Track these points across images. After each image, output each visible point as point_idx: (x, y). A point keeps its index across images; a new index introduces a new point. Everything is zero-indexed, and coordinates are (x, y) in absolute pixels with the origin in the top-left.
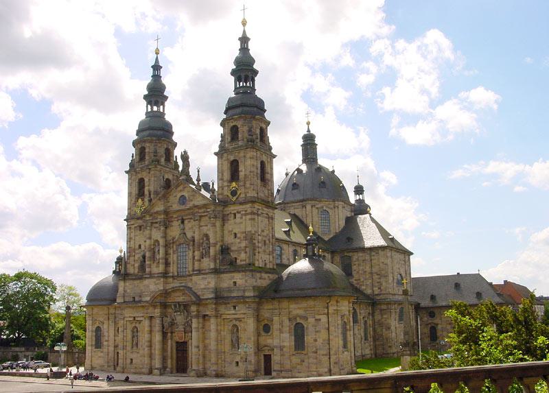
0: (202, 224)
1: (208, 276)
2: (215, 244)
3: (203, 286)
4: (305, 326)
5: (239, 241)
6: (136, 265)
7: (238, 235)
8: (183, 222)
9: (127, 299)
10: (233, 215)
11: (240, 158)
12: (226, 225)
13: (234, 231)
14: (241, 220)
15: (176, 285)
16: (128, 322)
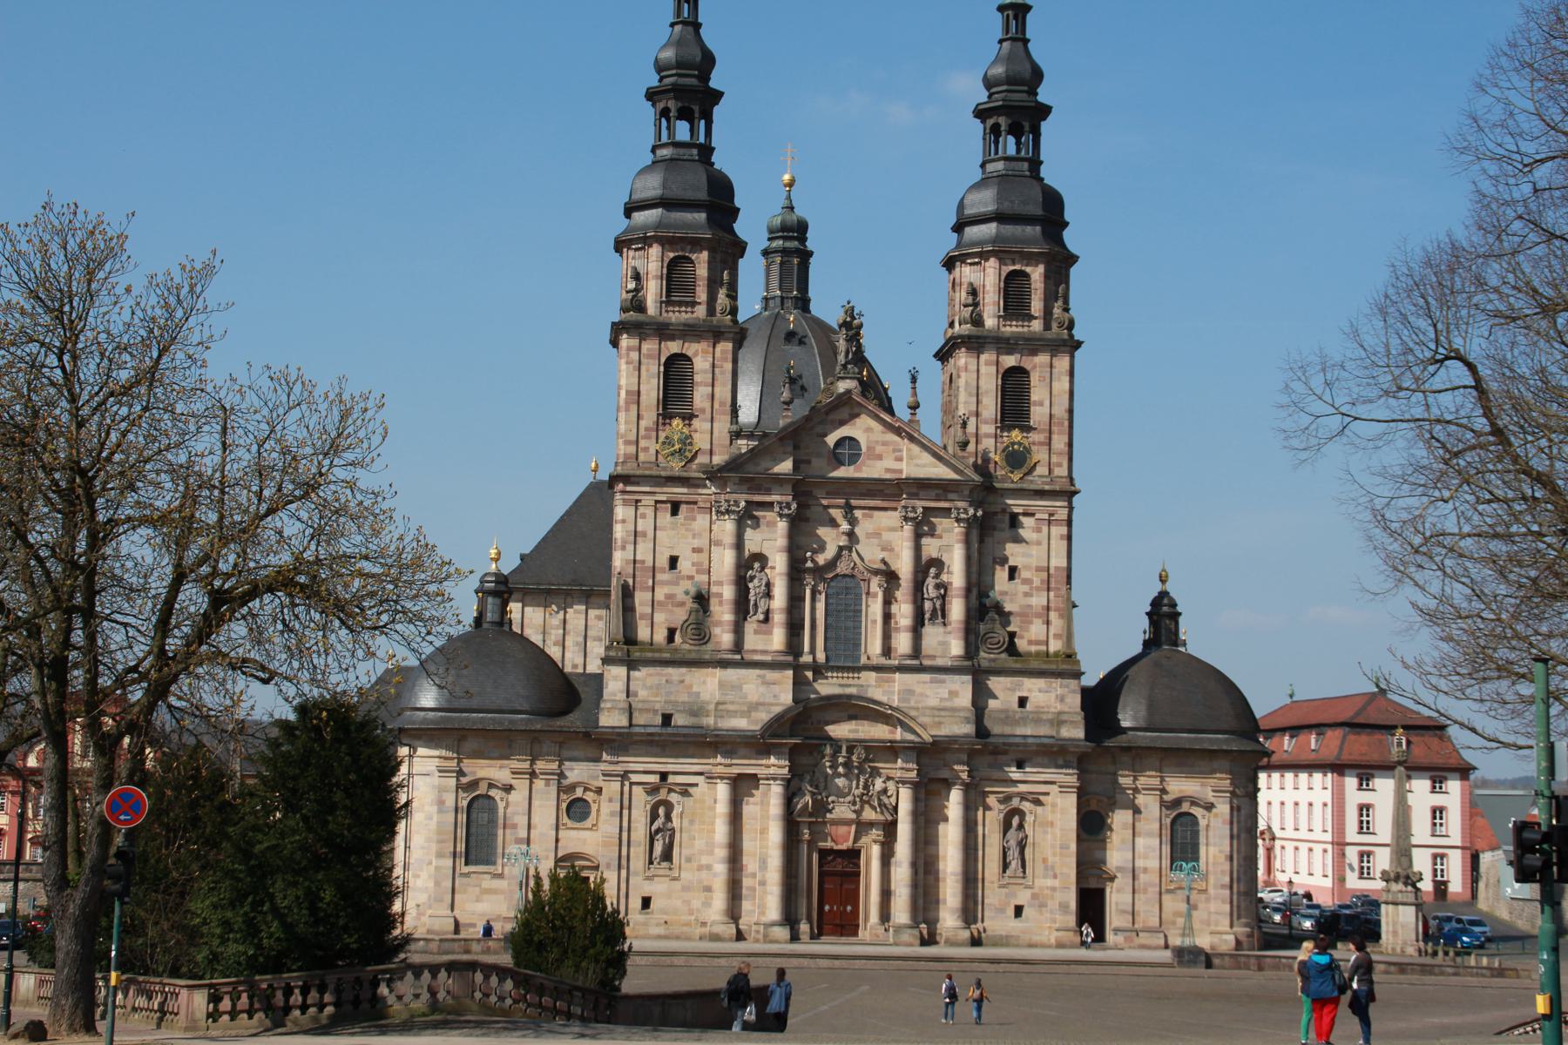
4: (1202, 823)
5: (1026, 588)
7: (1025, 574)
9: (639, 719)
10: (1007, 518)
11: (1035, 367)
12: (986, 539)
16: (637, 790)
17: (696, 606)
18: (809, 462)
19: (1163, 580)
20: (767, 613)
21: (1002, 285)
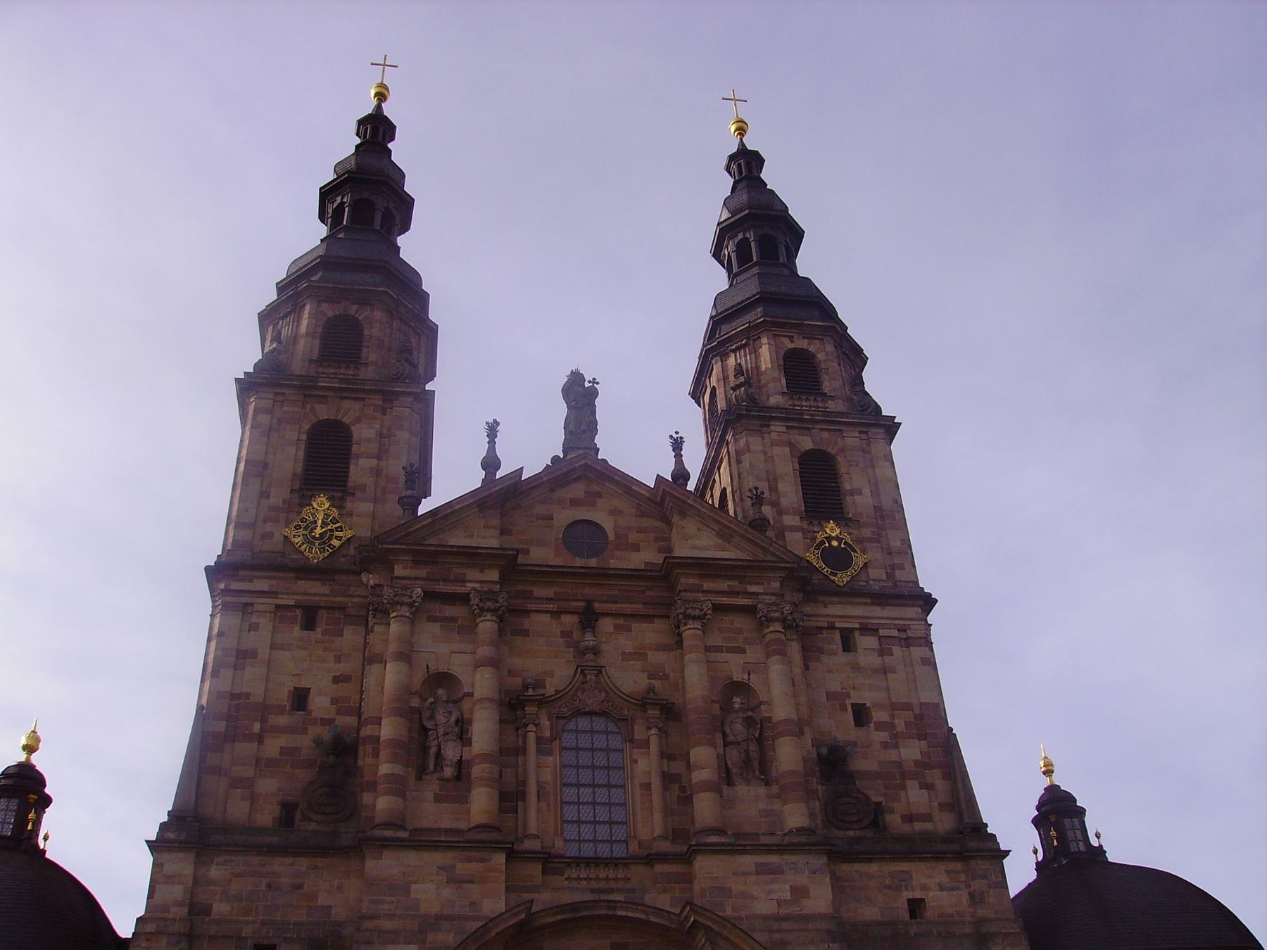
0: (716, 639)
1: (790, 858)
2: (798, 728)
3: (764, 907)
5: (884, 736)
6: (268, 785)
7: (880, 716)
8: (589, 618)
10: (837, 637)
11: (842, 450)
13: (856, 698)
14: (887, 659)
15: (567, 898)
17: (332, 759)
18: (527, 552)
19: (1048, 773)
20: (462, 766)
21: (782, 362)
